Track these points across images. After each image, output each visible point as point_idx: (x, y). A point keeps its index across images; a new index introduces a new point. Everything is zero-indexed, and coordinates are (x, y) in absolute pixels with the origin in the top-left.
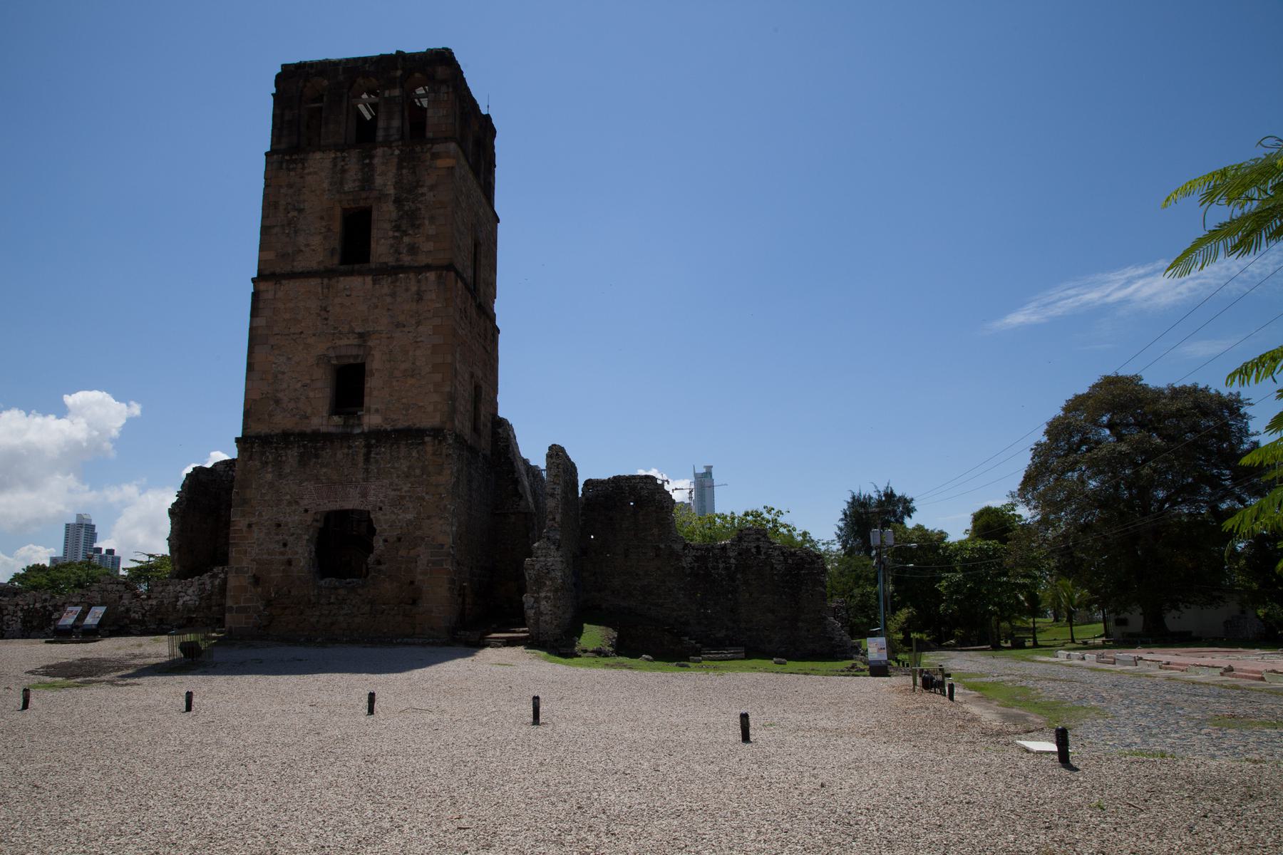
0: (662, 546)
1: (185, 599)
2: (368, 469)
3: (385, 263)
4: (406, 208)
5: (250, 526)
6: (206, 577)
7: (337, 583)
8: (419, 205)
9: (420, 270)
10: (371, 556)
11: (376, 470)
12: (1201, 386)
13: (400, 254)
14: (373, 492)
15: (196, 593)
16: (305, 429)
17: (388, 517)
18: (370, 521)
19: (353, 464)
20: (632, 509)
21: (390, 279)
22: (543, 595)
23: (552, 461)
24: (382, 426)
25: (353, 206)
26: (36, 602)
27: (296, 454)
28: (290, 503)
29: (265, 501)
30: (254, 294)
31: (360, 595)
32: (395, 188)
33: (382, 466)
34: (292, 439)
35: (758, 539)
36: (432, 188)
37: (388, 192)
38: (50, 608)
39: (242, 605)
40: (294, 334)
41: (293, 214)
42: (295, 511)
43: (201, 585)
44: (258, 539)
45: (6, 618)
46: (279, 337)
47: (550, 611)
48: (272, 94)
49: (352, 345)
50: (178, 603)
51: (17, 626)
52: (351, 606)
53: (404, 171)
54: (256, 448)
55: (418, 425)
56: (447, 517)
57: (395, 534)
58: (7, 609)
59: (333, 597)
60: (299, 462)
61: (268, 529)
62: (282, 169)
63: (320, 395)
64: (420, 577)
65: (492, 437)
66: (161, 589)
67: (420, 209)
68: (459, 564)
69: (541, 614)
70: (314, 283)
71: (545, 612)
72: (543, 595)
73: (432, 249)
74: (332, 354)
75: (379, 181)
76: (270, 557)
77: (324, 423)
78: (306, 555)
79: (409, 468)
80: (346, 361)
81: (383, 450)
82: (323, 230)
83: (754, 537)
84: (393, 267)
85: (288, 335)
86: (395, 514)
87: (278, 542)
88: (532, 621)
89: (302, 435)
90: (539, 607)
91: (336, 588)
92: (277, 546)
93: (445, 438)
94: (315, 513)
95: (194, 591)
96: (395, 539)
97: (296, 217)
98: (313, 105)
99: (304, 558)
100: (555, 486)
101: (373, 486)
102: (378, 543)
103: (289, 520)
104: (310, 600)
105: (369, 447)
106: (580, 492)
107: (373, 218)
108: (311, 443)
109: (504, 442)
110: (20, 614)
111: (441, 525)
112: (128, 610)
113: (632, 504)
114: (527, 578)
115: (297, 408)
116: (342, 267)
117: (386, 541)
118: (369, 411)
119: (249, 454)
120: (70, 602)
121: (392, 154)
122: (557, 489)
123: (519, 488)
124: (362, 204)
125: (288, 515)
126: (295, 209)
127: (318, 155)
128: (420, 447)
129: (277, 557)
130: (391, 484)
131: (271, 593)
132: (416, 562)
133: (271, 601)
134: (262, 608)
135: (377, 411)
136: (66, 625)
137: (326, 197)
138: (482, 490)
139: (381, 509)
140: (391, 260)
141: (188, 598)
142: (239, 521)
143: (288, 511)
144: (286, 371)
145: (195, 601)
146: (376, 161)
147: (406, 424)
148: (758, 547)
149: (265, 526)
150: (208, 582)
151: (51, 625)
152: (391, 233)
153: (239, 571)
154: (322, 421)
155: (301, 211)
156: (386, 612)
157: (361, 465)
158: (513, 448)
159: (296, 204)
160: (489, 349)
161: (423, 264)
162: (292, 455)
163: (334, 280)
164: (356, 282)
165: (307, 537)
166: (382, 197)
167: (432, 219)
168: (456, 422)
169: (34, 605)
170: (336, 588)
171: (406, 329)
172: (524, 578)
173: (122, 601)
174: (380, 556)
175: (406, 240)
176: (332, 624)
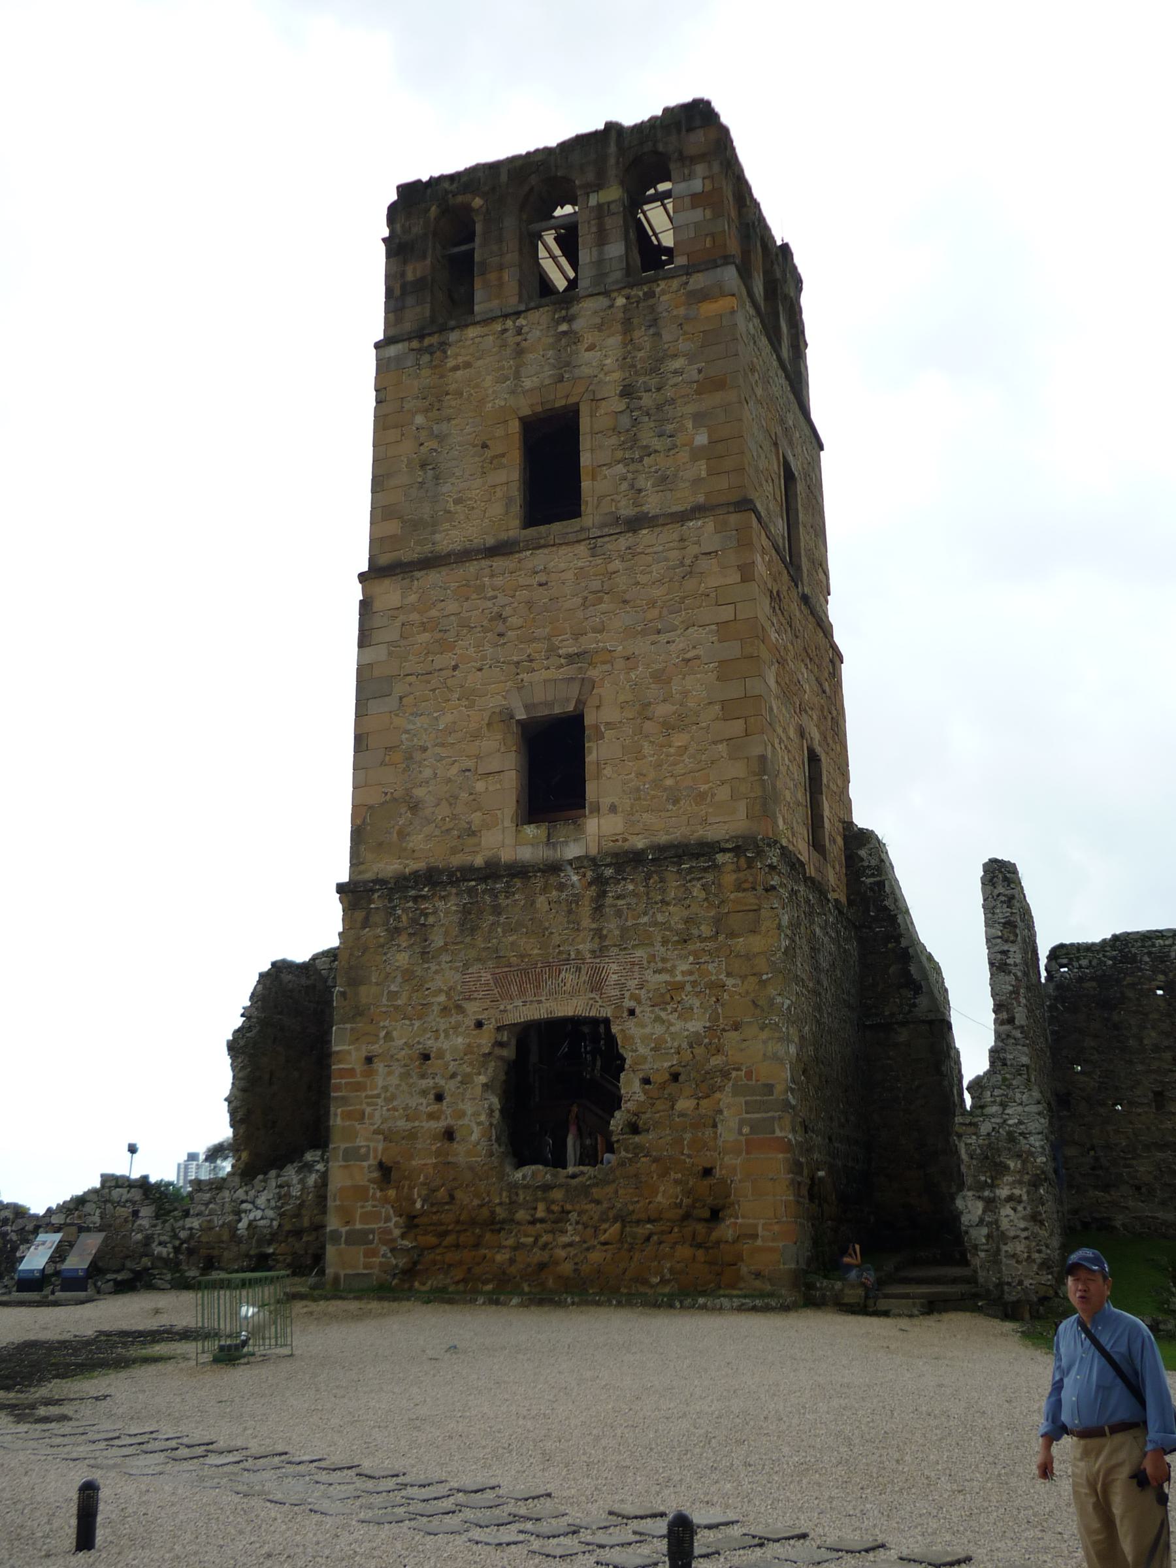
1: (251, 1216)
2: (601, 929)
4: (647, 400)
5: (369, 1060)
6: (291, 1173)
7: (548, 1176)
9: (682, 517)
10: (617, 1114)
11: (617, 932)
14: (615, 977)
15: (273, 1203)
17: (648, 1030)
18: (611, 1039)
19: (568, 922)
20: (1163, 1004)
22: (1004, 1192)
23: (996, 892)
24: (625, 840)
25: (539, 409)
27: (454, 908)
28: (445, 1010)
29: (397, 1008)
30: (361, 602)
31: (598, 1202)
38: (14, 1237)
39: (358, 1226)
40: (441, 670)
42: (455, 1028)
43: (280, 1186)
44: (385, 1088)
46: (412, 679)
47: (1025, 1229)
48: (384, 240)
50: (240, 1225)
52: (580, 1227)
53: (637, 334)
56: (776, 1024)
57: (666, 1065)
59: (541, 1207)
60: (462, 924)
61: (405, 1066)
65: (847, 867)
68: (806, 1129)
69: (1003, 1238)
71: (1012, 1233)
72: (1004, 1192)
73: (704, 474)
76: (409, 1125)
78: (483, 1118)
79: (687, 921)
81: (631, 887)
86: (663, 1022)
87: (424, 1093)
88: (982, 1255)
90: (996, 1222)
91: (547, 1188)
92: (425, 1102)
93: (760, 853)
94: (498, 1029)
95: (269, 1200)
96: (667, 1076)
97: (436, 450)
98: (456, 250)
99: (479, 1124)
100: (1006, 948)
101: (614, 967)
102: (631, 1087)
103: (446, 1045)
104: (493, 1213)
105: (599, 881)
106: (1044, 974)
109: (873, 875)
111: (765, 1042)
112: (148, 1240)
113: (1160, 992)
114: (964, 1156)
115: (454, 817)
117: (646, 1081)
118: (597, 809)
120: (47, 1224)
122: (1011, 954)
123: (913, 969)
125: (442, 1035)
127: (472, 332)
128: (710, 877)
129: (424, 1124)
131: (414, 1202)
132: (715, 1126)
133: (415, 1217)
134: (397, 1232)
136: (32, 1271)
138: (838, 973)
139: (632, 1012)
141: (259, 1214)
143: (442, 1027)
145: (272, 1220)
149: (398, 1060)
150: (295, 1179)
152: (619, 454)
153: (352, 1155)
155: (441, 438)
156: (655, 1238)
157: (586, 922)
158: (891, 886)
159: (435, 427)
160: (826, 686)
165: (482, 1079)
168: (780, 822)
171: (663, 638)
172: (956, 1152)
173: (139, 1222)
174: (635, 1114)
176: (542, 1266)
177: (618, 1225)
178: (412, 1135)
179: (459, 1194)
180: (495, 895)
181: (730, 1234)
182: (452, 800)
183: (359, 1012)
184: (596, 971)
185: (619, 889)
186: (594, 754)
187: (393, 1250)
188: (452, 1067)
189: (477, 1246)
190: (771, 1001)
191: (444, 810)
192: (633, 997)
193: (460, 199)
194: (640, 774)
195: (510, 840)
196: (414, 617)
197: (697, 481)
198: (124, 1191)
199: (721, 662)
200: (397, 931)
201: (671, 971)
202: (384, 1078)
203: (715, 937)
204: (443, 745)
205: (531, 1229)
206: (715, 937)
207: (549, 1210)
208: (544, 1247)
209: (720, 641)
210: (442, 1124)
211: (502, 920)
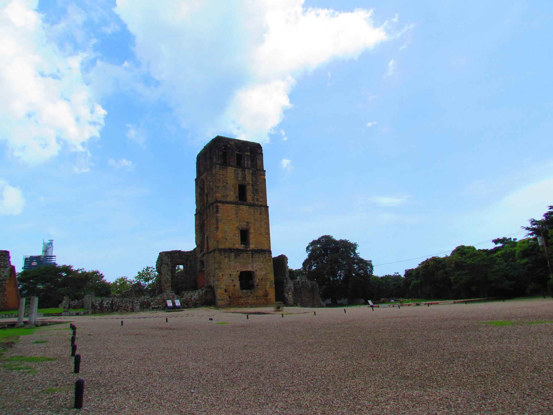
1: (194, 297)
3: (251, 203)
5: (222, 275)
6: (200, 290)
12: (347, 240)
13: (254, 200)
16: (234, 248)
21: (253, 208)
22: (290, 293)
25: (241, 184)
26: (144, 299)
28: (233, 269)
31: (253, 294)
33: (256, 259)
35: (305, 279)
36: (261, 183)
37: (250, 182)
38: (150, 301)
39: (222, 298)
40: (229, 220)
43: (199, 293)
44: (225, 279)
45: (135, 304)
49: (245, 225)
51: (138, 307)
53: (254, 177)
54: (222, 253)
58: (134, 302)
59: (247, 295)
60: (235, 257)
62: (220, 169)
63: (238, 238)
64: (268, 289)
66: (186, 294)
67: (258, 189)
70: (233, 205)
74: (240, 227)
75: (247, 178)
77: (240, 246)
79: (263, 260)
80: (244, 229)
82: (233, 190)
83: (304, 278)
84: (253, 204)
85: (228, 220)
87: (231, 280)
89: (234, 249)
103: (233, 273)
104: (241, 296)
105: (252, 254)
108: (237, 252)
110: (139, 303)
115: (232, 242)
116: (239, 202)
117: (259, 279)
119: (220, 254)
121: (250, 171)
124: (244, 184)
126: (225, 183)
127: (230, 168)
128: (265, 255)
130: (259, 264)
131: (230, 295)
134: (228, 299)
137: (234, 180)
139: (257, 271)
140: (252, 202)
141: (195, 297)
144: (228, 230)
146: (246, 173)
148: (305, 281)
150: (201, 292)
151: (150, 307)
152: (252, 194)
153: (221, 288)
154: (238, 245)
155: (227, 183)
161: (260, 204)
162: (233, 254)
163: (238, 206)
166: (249, 184)
167: (261, 192)
169: (144, 300)
170: (247, 293)
173: (174, 298)
175: (255, 197)
176: (247, 303)
178: (229, 286)
179: (236, 294)
180: (239, 254)
182: (232, 239)
183: (220, 268)
184: (253, 265)
185: (255, 255)
187: (227, 301)
188: (235, 276)
189: (238, 300)
190: (272, 271)
191: (230, 241)
192: (257, 269)
193: (226, 144)
194: (256, 240)
195: (240, 246)
196: (224, 210)
198: (171, 293)
199: (266, 227)
201: (261, 266)
202: (225, 278)
203: (266, 262)
204: (230, 231)
205: (245, 298)
206: (266, 262)
207: (247, 296)
208: (247, 300)
209: (265, 224)
210: (233, 284)
211: (240, 257)
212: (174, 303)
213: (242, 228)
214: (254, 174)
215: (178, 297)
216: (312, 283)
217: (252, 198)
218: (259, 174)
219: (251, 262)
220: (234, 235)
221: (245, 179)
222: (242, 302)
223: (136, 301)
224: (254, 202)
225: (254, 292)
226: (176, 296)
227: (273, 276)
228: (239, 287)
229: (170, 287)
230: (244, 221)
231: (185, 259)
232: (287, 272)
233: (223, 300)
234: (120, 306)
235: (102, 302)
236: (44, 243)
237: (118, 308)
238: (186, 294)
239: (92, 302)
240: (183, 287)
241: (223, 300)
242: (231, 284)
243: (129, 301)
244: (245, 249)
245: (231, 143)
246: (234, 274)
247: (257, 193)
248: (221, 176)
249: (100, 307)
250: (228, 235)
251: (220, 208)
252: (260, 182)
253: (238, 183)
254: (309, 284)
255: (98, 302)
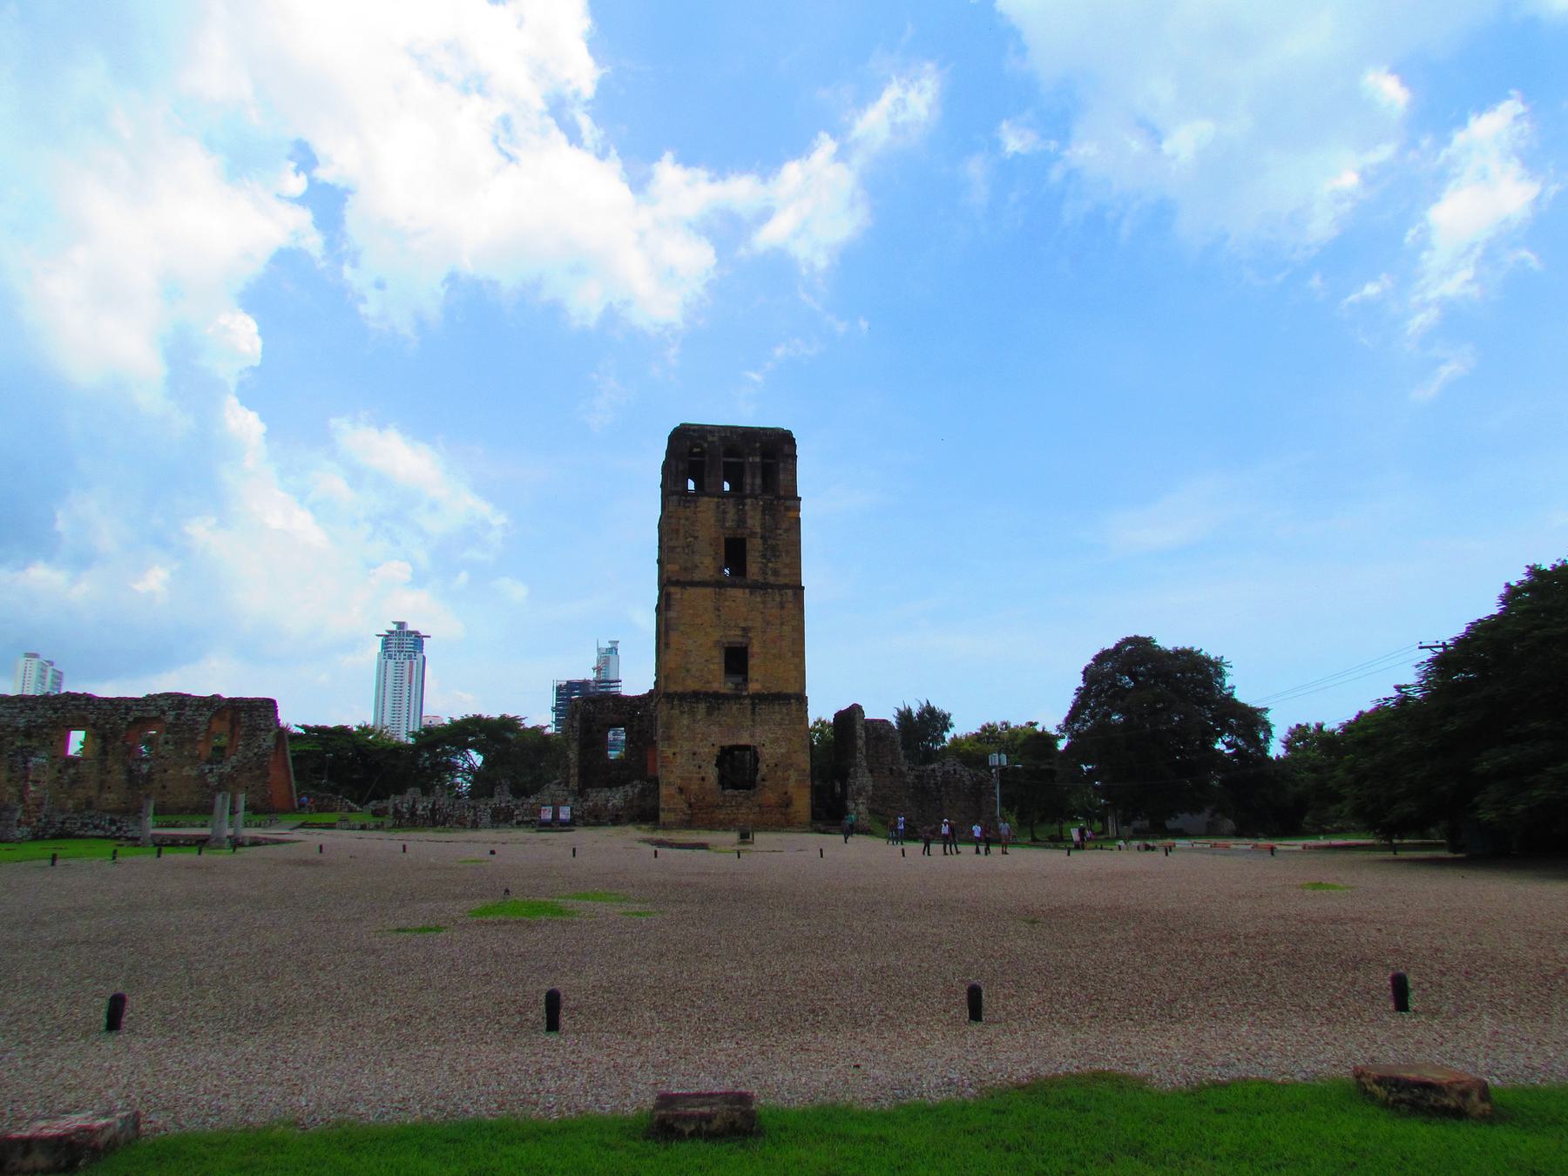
0: (894, 768)
5: (674, 754)
6: (628, 787)
8: (778, 542)
13: (767, 574)
21: (762, 592)
26: (501, 802)
31: (752, 801)
32: (761, 528)
33: (763, 718)
34: (701, 696)
36: (786, 531)
38: (513, 807)
39: (672, 806)
41: (689, 539)
44: (681, 763)
51: (487, 819)
54: (676, 702)
55: (784, 691)
58: (479, 807)
63: (717, 665)
66: (595, 794)
67: (778, 545)
70: (708, 590)
74: (724, 640)
75: (750, 522)
79: (782, 719)
80: (733, 645)
82: (713, 553)
84: (762, 584)
85: (693, 625)
87: (695, 766)
91: (736, 796)
102: (763, 768)
103: (702, 750)
105: (754, 705)
107: (747, 548)
108: (715, 701)
115: (702, 676)
117: (767, 766)
121: (758, 504)
130: (770, 729)
134: (685, 809)
135: (757, 680)
139: (764, 745)
140: (760, 579)
142: (663, 748)
146: (747, 508)
147: (777, 691)
148: (955, 770)
150: (630, 790)
151: (513, 819)
152: (760, 560)
153: (669, 784)
154: (720, 683)
155: (696, 538)
157: (748, 716)
163: (723, 591)
164: (738, 593)
165: (714, 762)
166: (753, 534)
167: (787, 552)
171: (774, 627)
175: (770, 565)
176: (734, 819)
177: (758, 808)
178: (691, 779)
179: (706, 797)
181: (792, 811)
183: (669, 738)
186: (752, 662)
193: (698, 442)
195: (722, 686)
197: (786, 575)
200: (684, 712)
202: (679, 759)
205: (730, 808)
212: (556, 813)
213: (729, 643)
214: (768, 509)
215: (575, 800)
216: (976, 775)
217: (761, 569)
218: (782, 508)
219: (751, 723)
220: (707, 661)
221: (745, 522)
222: (722, 817)
223: (481, 806)
224: (765, 579)
225: (753, 796)
226: (571, 799)
227: (809, 759)
228: (716, 782)
229: (576, 778)
230: (737, 626)
231: (629, 714)
232: (859, 749)
233: (674, 810)
234: (449, 815)
235: (413, 806)
236: (599, 649)
237: (445, 819)
238: (595, 794)
239: (395, 805)
240: (622, 777)
241: (674, 810)
242: (695, 775)
243: (469, 806)
244: (736, 692)
245: (710, 439)
246: (705, 752)
247: (775, 556)
248: (682, 521)
249: (410, 815)
250: (692, 660)
251: (675, 596)
252: (785, 526)
253: (724, 535)
254: (967, 778)
255: (406, 805)
